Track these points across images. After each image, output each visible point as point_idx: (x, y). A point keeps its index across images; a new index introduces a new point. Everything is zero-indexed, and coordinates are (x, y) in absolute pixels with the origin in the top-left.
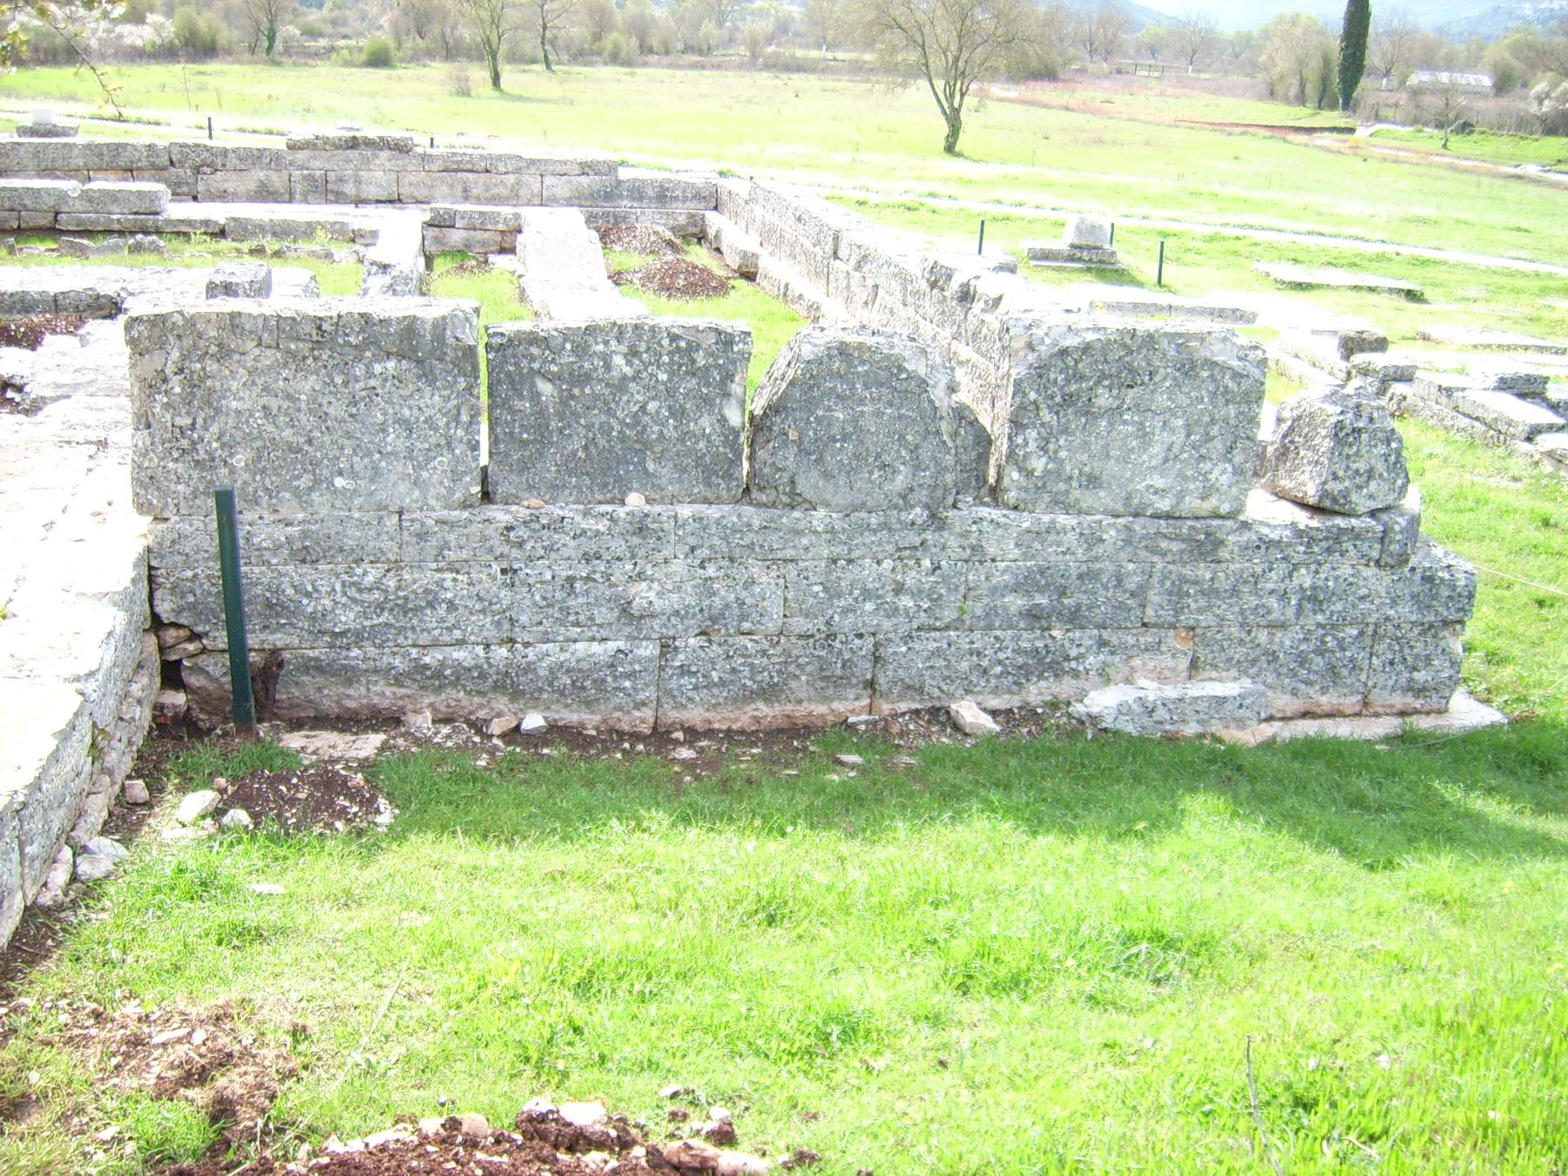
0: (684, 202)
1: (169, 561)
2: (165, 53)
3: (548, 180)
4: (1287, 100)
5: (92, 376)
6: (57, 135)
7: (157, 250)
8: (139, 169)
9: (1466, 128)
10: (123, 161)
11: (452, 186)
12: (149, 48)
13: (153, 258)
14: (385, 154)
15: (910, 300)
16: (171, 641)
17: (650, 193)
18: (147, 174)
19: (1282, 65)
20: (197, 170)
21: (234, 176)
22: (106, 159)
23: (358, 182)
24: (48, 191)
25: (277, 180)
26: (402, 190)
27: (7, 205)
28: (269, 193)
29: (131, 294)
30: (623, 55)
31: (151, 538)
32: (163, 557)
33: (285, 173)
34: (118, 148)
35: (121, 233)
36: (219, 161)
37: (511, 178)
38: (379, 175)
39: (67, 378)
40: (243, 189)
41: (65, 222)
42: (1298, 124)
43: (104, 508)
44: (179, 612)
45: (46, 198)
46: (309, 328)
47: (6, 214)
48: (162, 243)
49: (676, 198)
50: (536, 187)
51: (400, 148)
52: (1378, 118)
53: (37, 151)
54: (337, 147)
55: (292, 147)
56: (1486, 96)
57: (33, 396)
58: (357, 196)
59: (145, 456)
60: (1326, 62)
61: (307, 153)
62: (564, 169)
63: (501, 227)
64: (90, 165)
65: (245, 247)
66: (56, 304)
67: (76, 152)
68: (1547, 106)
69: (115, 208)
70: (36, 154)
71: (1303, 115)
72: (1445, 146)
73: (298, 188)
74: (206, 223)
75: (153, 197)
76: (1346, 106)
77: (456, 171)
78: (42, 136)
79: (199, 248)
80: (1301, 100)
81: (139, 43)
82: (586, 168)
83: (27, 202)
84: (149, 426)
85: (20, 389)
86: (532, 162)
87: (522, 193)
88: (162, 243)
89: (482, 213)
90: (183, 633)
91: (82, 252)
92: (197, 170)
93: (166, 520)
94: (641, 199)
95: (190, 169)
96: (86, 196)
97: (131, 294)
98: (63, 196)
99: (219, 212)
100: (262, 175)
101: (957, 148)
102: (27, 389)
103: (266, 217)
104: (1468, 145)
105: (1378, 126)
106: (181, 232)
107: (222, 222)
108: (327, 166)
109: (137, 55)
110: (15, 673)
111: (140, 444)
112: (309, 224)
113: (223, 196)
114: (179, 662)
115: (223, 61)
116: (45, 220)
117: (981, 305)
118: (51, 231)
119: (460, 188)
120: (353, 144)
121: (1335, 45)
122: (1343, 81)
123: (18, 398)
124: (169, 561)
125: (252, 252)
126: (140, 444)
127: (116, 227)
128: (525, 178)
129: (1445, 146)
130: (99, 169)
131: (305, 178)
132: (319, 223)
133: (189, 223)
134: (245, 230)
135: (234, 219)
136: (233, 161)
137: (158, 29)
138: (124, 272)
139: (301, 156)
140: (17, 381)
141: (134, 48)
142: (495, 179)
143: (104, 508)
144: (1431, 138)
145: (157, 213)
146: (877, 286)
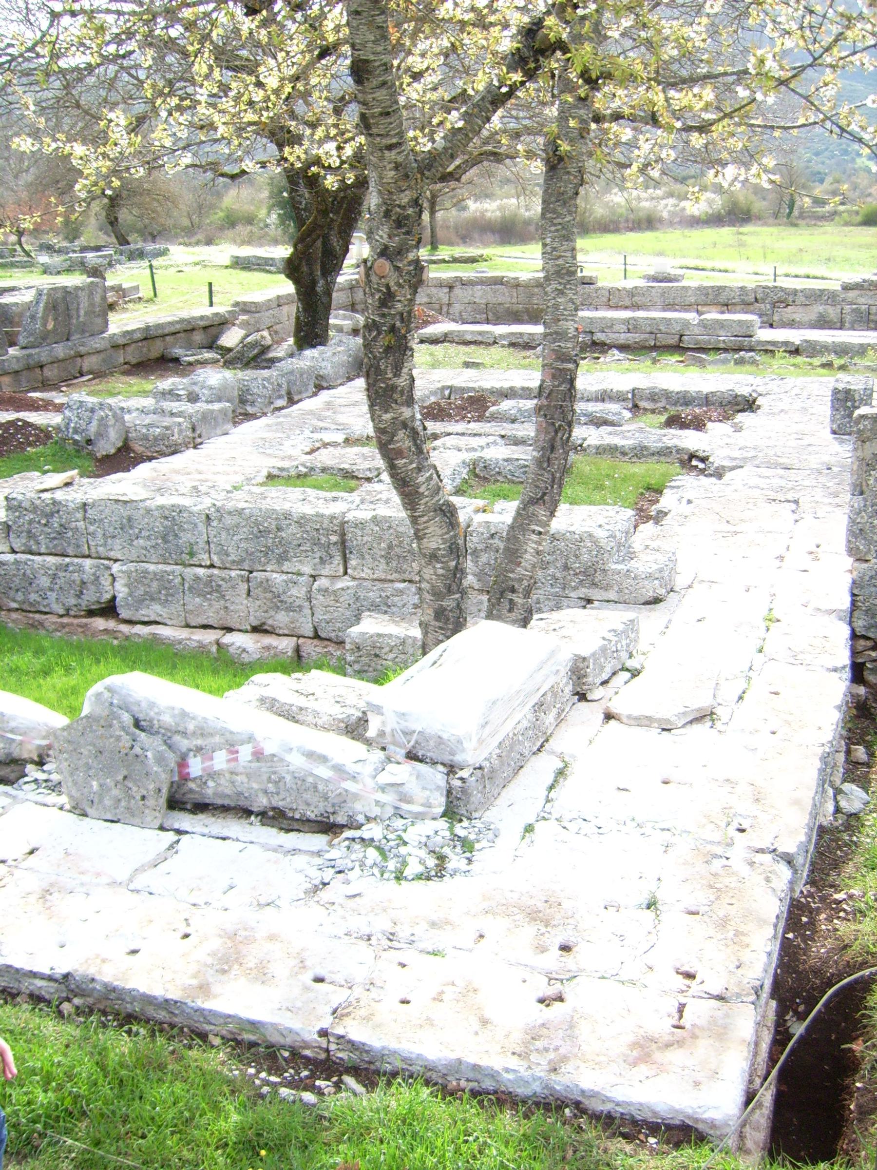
1: (866, 591)
2: (715, 220)
5: (752, 453)
6: (670, 281)
7: (754, 362)
10: (723, 298)
12: (703, 217)
13: (752, 368)
16: (860, 648)
18: (738, 308)
20: (774, 305)
21: (801, 309)
22: (711, 297)
24: (676, 320)
25: (832, 313)
27: (648, 330)
28: (825, 322)
29: (760, 395)
31: (855, 573)
32: (862, 588)
34: (720, 289)
35: (726, 350)
36: (791, 299)
39: (737, 454)
40: (806, 319)
41: (687, 342)
43: (814, 549)
44: (868, 628)
45: (675, 325)
47: (647, 336)
48: (758, 358)
53: (664, 293)
55: (846, 288)
57: (716, 465)
59: (858, 514)
64: (699, 301)
65: (817, 361)
66: (707, 400)
67: (690, 293)
69: (722, 333)
73: (848, 318)
74: (786, 343)
75: (749, 325)
78: (661, 281)
79: (781, 362)
81: (697, 213)
84: (862, 493)
85: (703, 460)
88: (758, 358)
90: (869, 644)
91: (702, 364)
92: (774, 305)
93: (867, 561)
95: (772, 303)
96: (703, 324)
97: (760, 395)
98: (686, 324)
99: (795, 336)
100: (821, 309)
102: (711, 460)
103: (830, 340)
106: (769, 350)
107: (797, 342)
109: (695, 222)
110: (792, 661)
111: (856, 505)
112: (861, 345)
113: (791, 324)
114: (864, 664)
115: (755, 225)
116: (673, 341)
118: (678, 348)
123: (701, 466)
124: (866, 591)
125: (823, 366)
126: (856, 505)
127: (722, 346)
130: (706, 305)
131: (853, 310)
132: (869, 345)
133: (773, 343)
134: (814, 349)
135: (806, 341)
136: (801, 299)
137: (710, 202)
138: (750, 379)
139: (851, 295)
140: (701, 454)
141: (693, 217)
143: (814, 549)
145: (751, 336)
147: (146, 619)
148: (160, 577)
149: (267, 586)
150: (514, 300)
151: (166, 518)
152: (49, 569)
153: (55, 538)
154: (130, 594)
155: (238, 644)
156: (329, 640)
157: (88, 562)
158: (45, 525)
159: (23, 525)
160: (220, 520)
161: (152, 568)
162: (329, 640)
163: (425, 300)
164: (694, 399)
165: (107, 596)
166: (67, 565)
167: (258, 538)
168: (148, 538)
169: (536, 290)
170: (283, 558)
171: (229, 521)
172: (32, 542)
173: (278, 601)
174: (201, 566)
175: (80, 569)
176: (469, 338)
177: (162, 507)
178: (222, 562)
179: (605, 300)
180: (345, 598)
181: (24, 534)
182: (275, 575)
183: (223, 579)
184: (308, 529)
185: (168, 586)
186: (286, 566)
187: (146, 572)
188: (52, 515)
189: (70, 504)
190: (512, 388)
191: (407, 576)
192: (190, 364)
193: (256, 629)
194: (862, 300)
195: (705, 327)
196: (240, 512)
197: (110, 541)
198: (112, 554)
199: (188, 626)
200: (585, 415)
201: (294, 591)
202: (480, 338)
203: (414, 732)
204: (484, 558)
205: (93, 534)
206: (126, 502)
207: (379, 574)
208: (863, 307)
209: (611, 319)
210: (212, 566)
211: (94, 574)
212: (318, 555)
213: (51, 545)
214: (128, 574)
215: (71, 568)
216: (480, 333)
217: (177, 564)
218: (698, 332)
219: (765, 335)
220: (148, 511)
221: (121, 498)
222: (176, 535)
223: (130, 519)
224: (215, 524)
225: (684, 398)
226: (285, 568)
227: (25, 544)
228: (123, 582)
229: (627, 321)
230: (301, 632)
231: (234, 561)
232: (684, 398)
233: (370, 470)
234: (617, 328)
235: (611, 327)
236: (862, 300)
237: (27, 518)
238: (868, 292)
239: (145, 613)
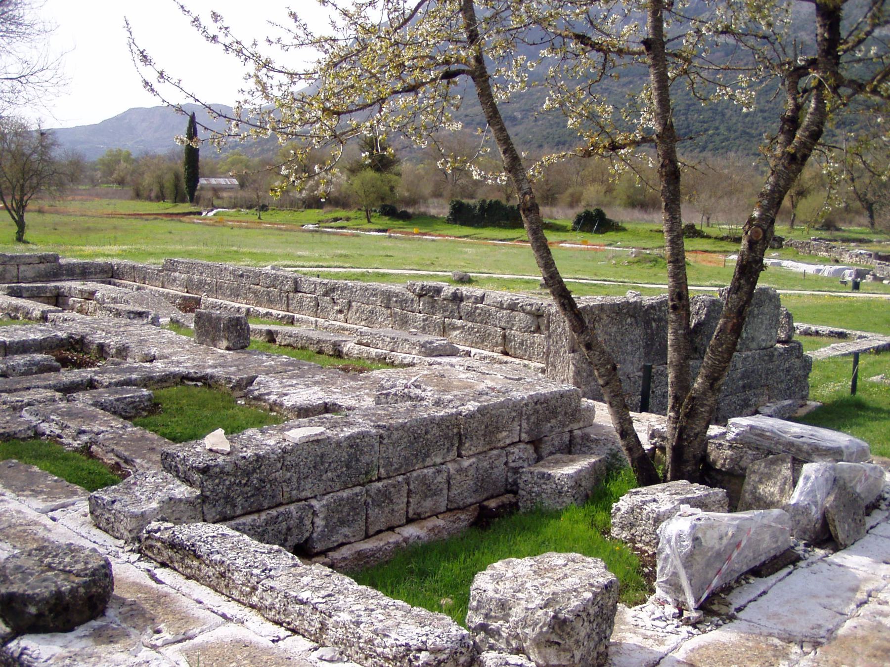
0: (95, 274)
3: (22, 268)
4: (149, 199)
9: (264, 208)
15: (392, 304)
17: (78, 271)
19: (147, 180)
42: (167, 211)
46: (616, 308)
49: (91, 273)
50: (15, 273)
52: (214, 207)
60: (177, 177)
62: (30, 261)
63: (48, 295)
68: (304, 194)
71: (167, 206)
72: (259, 218)
76: (192, 201)
80: (161, 197)
82: (43, 259)
84: (573, 352)
86: (12, 258)
87: (7, 276)
89: (37, 287)
101: (24, 238)
104: (269, 217)
105: (215, 211)
117: (473, 300)
121: (181, 168)
122: (188, 187)
128: (9, 267)
129: (259, 218)
144: (250, 216)
146: (350, 303)
147: (335, 544)
148: (350, 500)
149: (423, 479)
151: (351, 447)
152: (258, 527)
153: (252, 496)
154: (326, 526)
155: (415, 534)
156: (458, 508)
157: (292, 507)
158: (245, 484)
159: (222, 492)
160: (389, 437)
161: (345, 494)
162: (458, 508)
164: (30, 346)
165: (307, 534)
166: (277, 517)
167: (412, 443)
168: (335, 470)
170: (427, 455)
171: (395, 435)
172: (229, 507)
173: (429, 490)
174: (371, 481)
175: (288, 516)
177: (348, 437)
178: (387, 472)
180: (472, 472)
181: (222, 501)
182: (426, 471)
183: (394, 486)
184: (444, 427)
185: (356, 506)
186: (429, 462)
187: (342, 499)
188: (254, 470)
189: (272, 456)
191: (493, 445)
193: (410, 521)
196: (403, 426)
197: (303, 483)
198: (304, 494)
199: (367, 536)
200: (34, 365)
201: (439, 479)
203: (853, 453)
204: (533, 419)
205: (288, 481)
206: (318, 441)
207: (480, 449)
210: (379, 479)
211: (300, 517)
212: (447, 446)
213: (247, 505)
214: (327, 506)
215: (281, 519)
217: (354, 486)
220: (339, 444)
221: (320, 438)
222: (358, 460)
223: (322, 456)
224: (385, 441)
225: (23, 346)
226: (427, 464)
227: (220, 513)
228: (321, 516)
230: (439, 511)
231: (396, 469)
232: (23, 346)
233: (29, 429)
237: (227, 483)
239: (338, 538)
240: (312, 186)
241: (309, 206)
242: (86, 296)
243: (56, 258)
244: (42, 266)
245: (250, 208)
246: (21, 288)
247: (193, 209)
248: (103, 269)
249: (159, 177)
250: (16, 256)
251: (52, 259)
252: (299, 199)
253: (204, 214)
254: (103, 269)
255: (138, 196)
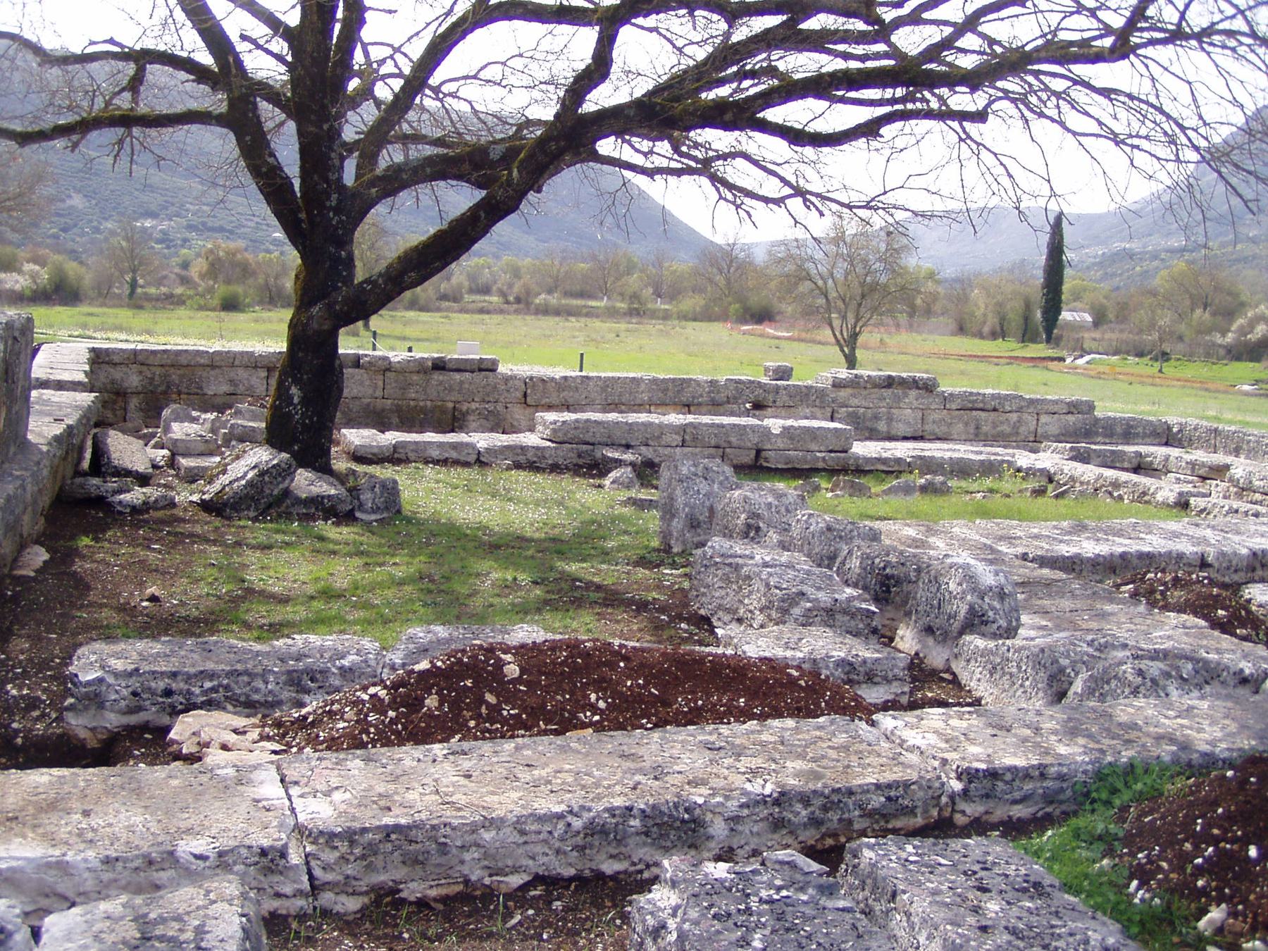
3: (1044, 419)
8: (699, 404)
9: (1165, 356)
11: (966, 424)
12: (28, 293)
14: (913, 393)
17: (1119, 430)
18: (705, 409)
22: (670, 394)
23: (890, 420)
26: (927, 427)
27: (713, 443)
30: (422, 302)
33: (830, 410)
37: (1014, 417)
38: (907, 412)
42: (1013, 354)
45: (751, 436)
49: (1137, 435)
51: (927, 387)
52: (1085, 352)
54: (876, 386)
56: (1089, 330)
58: (888, 432)
60: (1028, 306)
61: (849, 391)
63: (1126, 465)
67: (643, 386)
68: (1230, 338)
70: (604, 389)
72: (1160, 371)
76: (1048, 340)
77: (971, 409)
80: (999, 333)
81: (18, 287)
83: (733, 439)
86: (1032, 402)
94: (1111, 436)
103: (947, 455)
104: (1172, 370)
108: (864, 403)
119: (973, 426)
120: (890, 382)
127: (821, 465)
128: (1025, 416)
129: (1160, 371)
130: (664, 404)
136: (783, 398)
137: (34, 276)
139: (843, 394)
141: (13, 291)
142: (1003, 417)
144: (1145, 367)
150: (379, 393)
163: (225, 388)
169: (415, 378)
176: (435, 454)
179: (519, 395)
190: (1123, 556)
192: (135, 510)
194: (854, 402)
195: (792, 439)
202: (454, 455)
208: (862, 410)
209: (661, 426)
216: (455, 446)
218: (782, 446)
219: (864, 449)
229: (683, 428)
234: (668, 439)
235: (659, 437)
236: (854, 402)
238: (865, 392)
240: (1242, 327)
241: (1238, 358)
242: (1202, 472)
243: (1091, 407)
244: (1071, 418)
245: (1140, 354)
246: (1088, 451)
247: (1051, 353)
248: (1155, 430)
249: (1000, 304)
250: (1038, 400)
251: (1085, 408)
252: (1220, 346)
253: (1069, 360)
254: (1155, 430)
255: (961, 330)
